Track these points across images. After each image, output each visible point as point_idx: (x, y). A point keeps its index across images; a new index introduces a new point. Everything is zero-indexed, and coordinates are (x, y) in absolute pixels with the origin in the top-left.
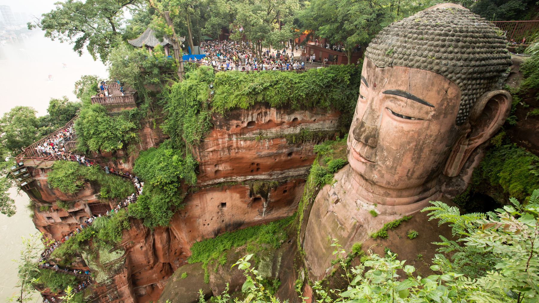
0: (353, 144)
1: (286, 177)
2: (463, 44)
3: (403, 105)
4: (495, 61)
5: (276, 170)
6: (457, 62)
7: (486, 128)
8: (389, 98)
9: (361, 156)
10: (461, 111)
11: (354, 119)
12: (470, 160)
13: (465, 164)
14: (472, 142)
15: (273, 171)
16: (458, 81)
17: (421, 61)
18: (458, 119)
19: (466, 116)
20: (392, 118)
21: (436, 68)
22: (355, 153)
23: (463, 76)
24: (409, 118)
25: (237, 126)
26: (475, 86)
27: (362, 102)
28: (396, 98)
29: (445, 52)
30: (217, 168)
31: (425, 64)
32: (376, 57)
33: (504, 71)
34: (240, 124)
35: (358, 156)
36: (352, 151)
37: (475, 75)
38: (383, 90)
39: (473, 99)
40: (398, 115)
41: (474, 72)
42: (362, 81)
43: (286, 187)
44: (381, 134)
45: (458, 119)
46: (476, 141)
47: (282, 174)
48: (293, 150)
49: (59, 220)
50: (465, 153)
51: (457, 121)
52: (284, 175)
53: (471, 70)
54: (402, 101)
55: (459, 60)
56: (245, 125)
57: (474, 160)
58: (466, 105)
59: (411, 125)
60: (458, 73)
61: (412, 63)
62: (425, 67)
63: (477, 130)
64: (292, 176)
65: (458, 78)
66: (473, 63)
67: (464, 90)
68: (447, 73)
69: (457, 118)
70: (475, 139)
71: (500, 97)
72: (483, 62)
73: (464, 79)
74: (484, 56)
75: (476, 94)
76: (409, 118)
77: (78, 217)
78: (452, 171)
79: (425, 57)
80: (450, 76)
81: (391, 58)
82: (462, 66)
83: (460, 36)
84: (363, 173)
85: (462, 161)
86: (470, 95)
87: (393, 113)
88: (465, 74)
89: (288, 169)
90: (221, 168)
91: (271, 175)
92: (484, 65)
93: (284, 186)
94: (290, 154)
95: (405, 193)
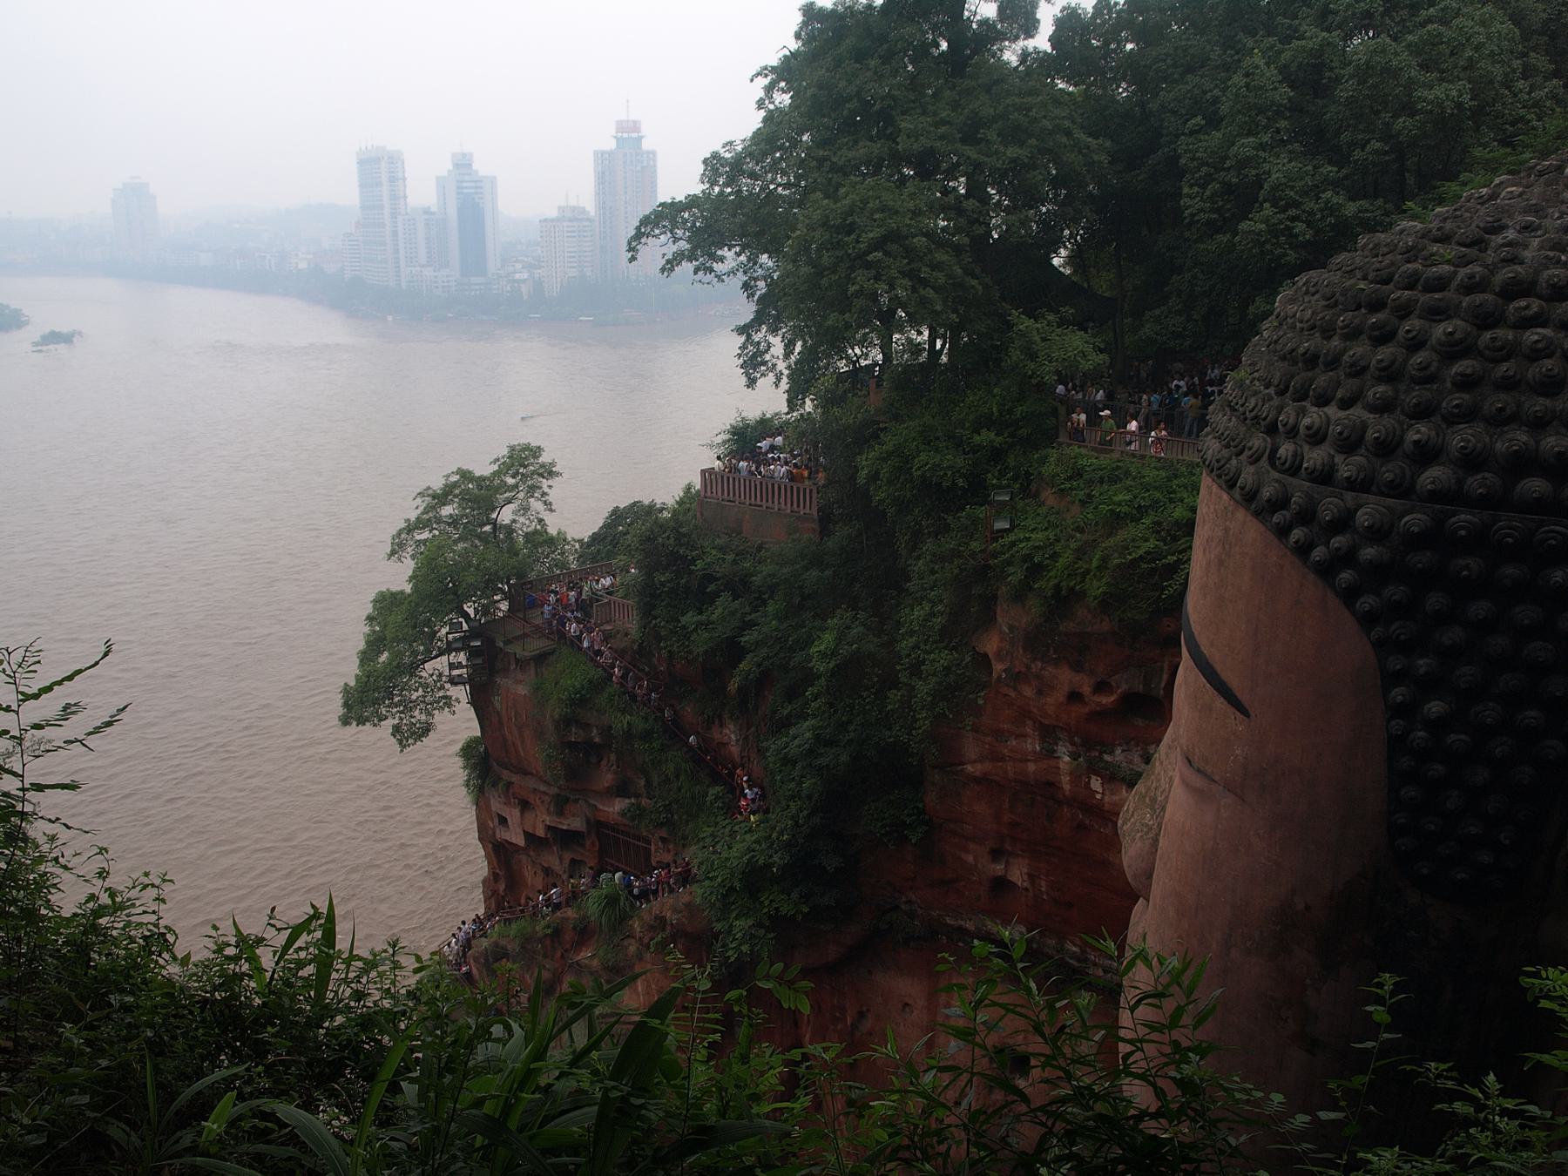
6: (1339, 459)
16: (1346, 576)
23: (1368, 553)
25: (1075, 696)
30: (999, 868)
34: (1086, 690)
37: (1470, 565)
49: (521, 842)
53: (1415, 520)
55: (1349, 445)
56: (1107, 700)
65: (1347, 558)
66: (1433, 476)
77: (568, 856)
80: (1297, 534)
88: (1377, 534)
90: (1018, 874)
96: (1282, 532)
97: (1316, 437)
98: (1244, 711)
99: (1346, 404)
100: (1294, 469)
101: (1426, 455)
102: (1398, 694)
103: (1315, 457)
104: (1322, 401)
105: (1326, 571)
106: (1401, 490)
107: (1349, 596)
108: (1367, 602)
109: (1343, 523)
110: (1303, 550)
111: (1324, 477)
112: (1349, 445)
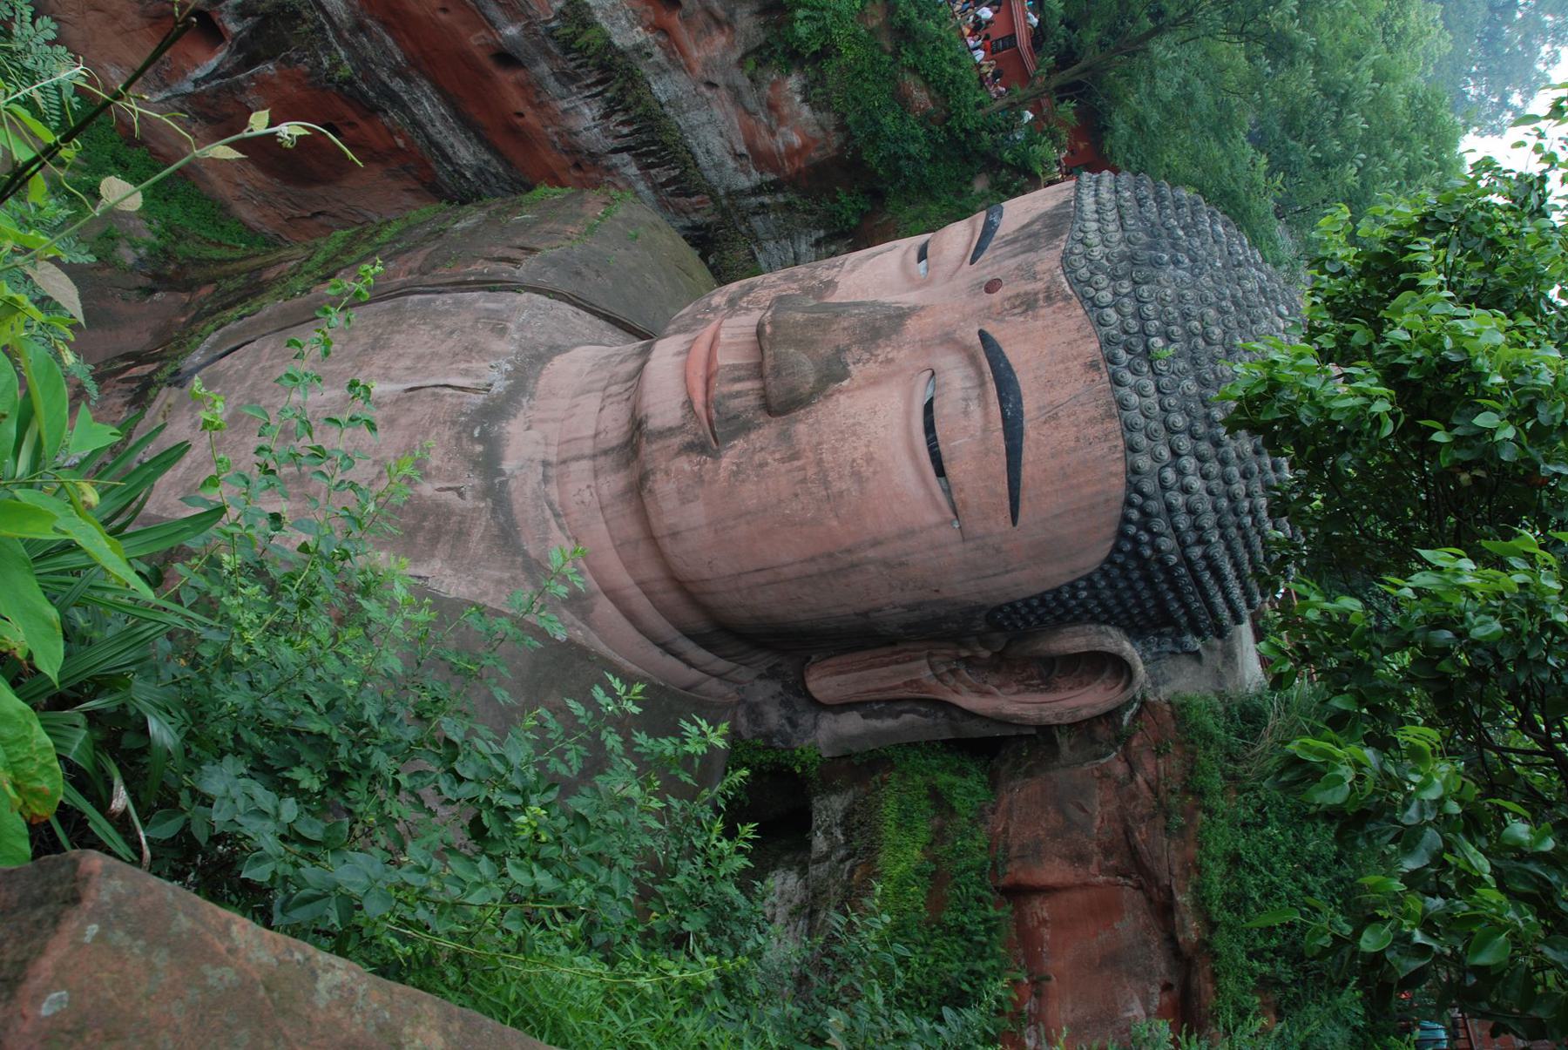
0: (727, 326)
1: (394, 98)
2: (1242, 493)
3: (970, 425)
4: (1219, 600)
5: (397, 41)
7: (1015, 689)
8: (973, 359)
9: (707, 381)
10: (1035, 603)
11: (823, 270)
12: (891, 705)
13: (871, 702)
14: (952, 682)
15: (386, 25)
16: (1128, 547)
17: (1146, 402)
18: (1007, 609)
19: (1028, 623)
20: (908, 414)
21: (1144, 462)
22: (702, 348)
23: (1148, 552)
24: (940, 471)
26: (1128, 594)
27: (904, 266)
28: (982, 384)
29: (1201, 458)
31: (1141, 421)
32: (1094, 238)
33: (1199, 633)
35: (701, 372)
36: (706, 334)
38: (990, 328)
39: (1087, 611)
40: (929, 428)
41: (1169, 571)
42: (980, 218)
43: (351, 125)
44: (831, 404)
45: (1007, 609)
46: (963, 688)
47: (397, 72)
48: (534, 62)
50: (905, 684)
51: (1000, 608)
52: (397, 84)
53: (1174, 559)
54: (986, 414)
57: (897, 715)
58: (1062, 604)
59: (921, 492)
60: (1149, 531)
61: (1129, 378)
62: (1129, 427)
63: (997, 669)
64: (417, 124)
65: (1135, 540)
66: (1196, 552)
67: (1105, 574)
68: (1137, 499)
69: (1012, 605)
70: (964, 682)
71: (1119, 667)
72: (1207, 575)
73: (1136, 554)
74: (1228, 568)
75: (1106, 609)
76: (940, 471)
78: (824, 683)
79: (1163, 409)
80: (1135, 515)
81: (1115, 294)
82: (1176, 529)
83: (1261, 471)
84: (654, 424)
85: (878, 690)
86: (1096, 597)
87: (929, 408)
89: (438, 88)
91: (360, 27)
92: (1198, 582)
93: (351, 115)
94: (506, 58)
95: (672, 598)
96: (1129, 503)
97: (1186, 490)
98: (1014, 524)
99: (1210, 492)
100: (1163, 486)
101: (1201, 541)
102: (1082, 584)
103: (1178, 500)
104: (1205, 477)
105: (1122, 534)
106: (1182, 544)
107: (1117, 549)
108: (1120, 559)
109: (1154, 535)
110: (1126, 520)
111: (1170, 508)
112: (1191, 511)
